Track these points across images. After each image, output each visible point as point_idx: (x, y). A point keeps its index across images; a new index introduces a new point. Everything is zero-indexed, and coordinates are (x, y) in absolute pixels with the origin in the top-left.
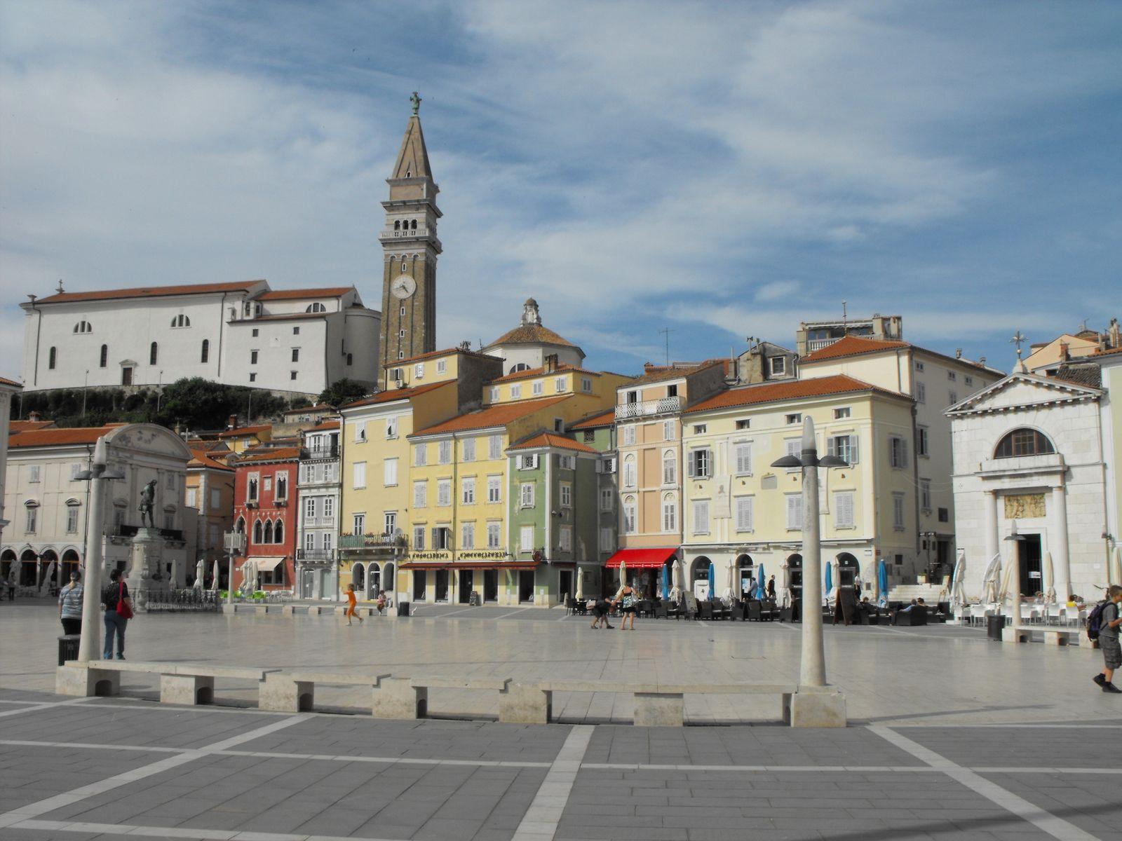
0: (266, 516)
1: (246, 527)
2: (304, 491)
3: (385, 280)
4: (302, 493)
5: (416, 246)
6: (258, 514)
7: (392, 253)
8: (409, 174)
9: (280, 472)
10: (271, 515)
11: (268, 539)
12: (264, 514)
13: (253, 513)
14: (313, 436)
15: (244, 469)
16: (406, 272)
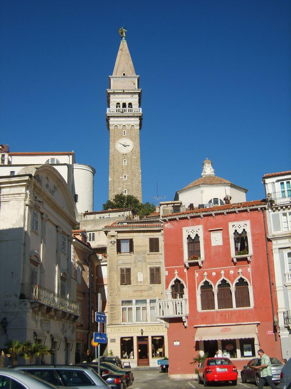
0: (219, 275)
1: (186, 290)
2: (279, 242)
4: (276, 245)
5: (133, 119)
6: (206, 274)
7: (116, 123)
8: (124, 74)
9: (236, 223)
10: (227, 274)
11: (225, 302)
12: (214, 274)
13: (197, 275)
14: (278, 181)
15: (175, 223)
16: (126, 137)
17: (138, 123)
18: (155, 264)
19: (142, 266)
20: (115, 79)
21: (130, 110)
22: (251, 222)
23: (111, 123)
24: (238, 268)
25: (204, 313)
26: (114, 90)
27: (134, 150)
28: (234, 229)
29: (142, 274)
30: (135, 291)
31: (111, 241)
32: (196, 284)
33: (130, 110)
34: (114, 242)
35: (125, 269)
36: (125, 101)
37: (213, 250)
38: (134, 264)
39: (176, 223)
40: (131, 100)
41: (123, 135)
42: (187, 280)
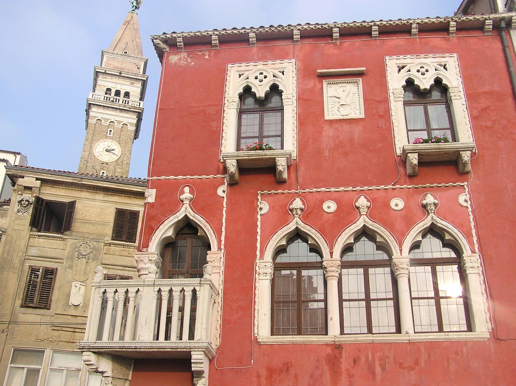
3: (87, 140)
7: (100, 116)
12: (330, 206)
13: (264, 207)
16: (111, 138)
17: (135, 121)
18: (122, 268)
19: (86, 269)
20: (110, 56)
21: (126, 101)
22: (461, 59)
23: (91, 114)
24: (425, 191)
25: (282, 346)
26: (106, 69)
27: (121, 159)
28: (403, 76)
29: (83, 288)
30: (56, 328)
31: (21, 199)
32: (259, 237)
33: (126, 101)
34: (27, 203)
35: (41, 268)
36: (120, 88)
37: (328, 132)
38: (66, 262)
39: (207, 53)
40: (129, 89)
41: (108, 135)
42: (224, 221)
